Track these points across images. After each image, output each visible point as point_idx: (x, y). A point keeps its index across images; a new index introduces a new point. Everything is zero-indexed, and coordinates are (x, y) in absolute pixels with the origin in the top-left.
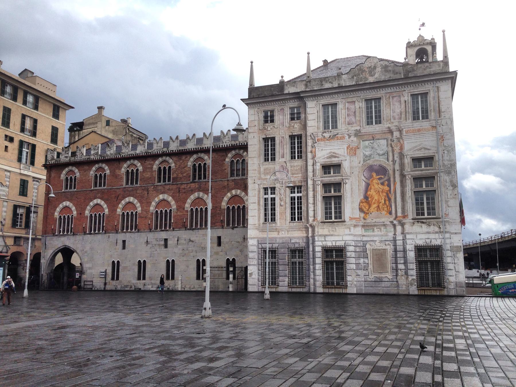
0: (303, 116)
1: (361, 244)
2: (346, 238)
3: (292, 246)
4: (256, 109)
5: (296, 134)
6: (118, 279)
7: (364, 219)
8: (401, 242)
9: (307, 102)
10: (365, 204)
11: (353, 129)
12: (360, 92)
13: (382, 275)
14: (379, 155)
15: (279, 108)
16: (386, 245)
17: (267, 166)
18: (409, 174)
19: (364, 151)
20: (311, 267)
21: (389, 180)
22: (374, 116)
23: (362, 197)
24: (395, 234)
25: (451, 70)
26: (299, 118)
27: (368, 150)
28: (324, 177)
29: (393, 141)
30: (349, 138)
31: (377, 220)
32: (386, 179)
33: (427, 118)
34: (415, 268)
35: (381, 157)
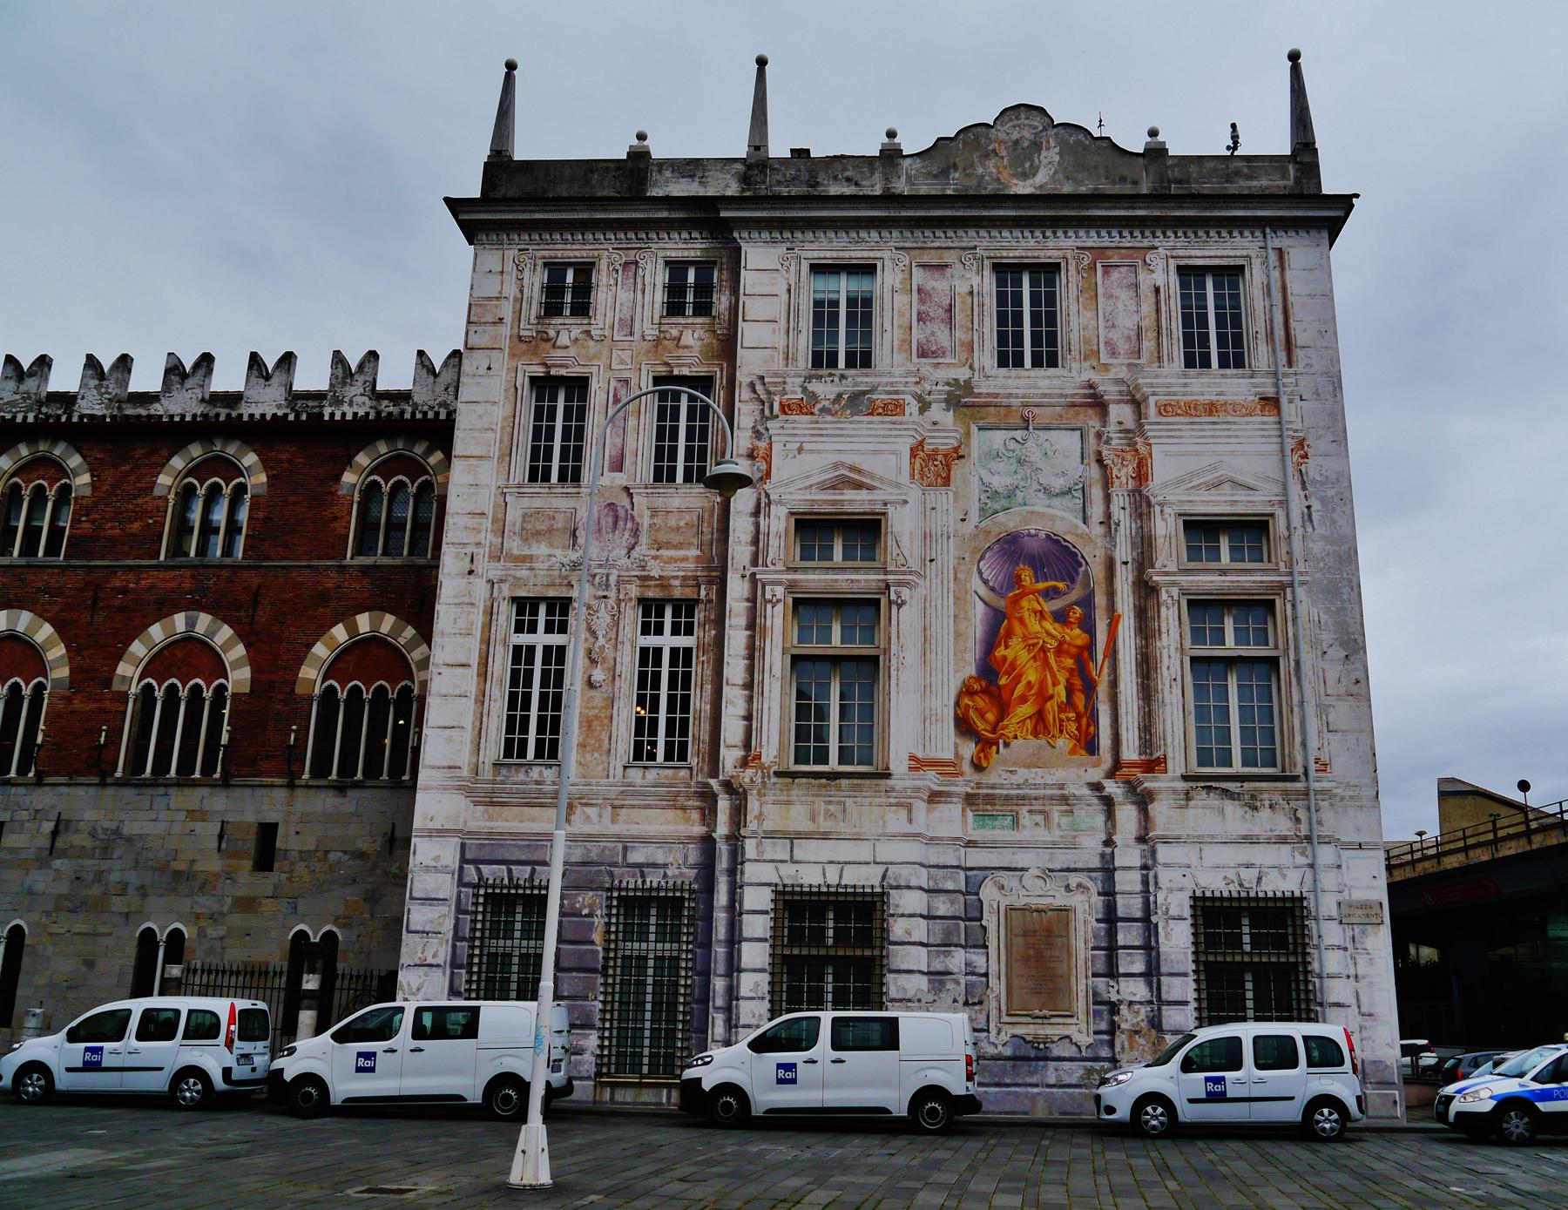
0: (721, 302)
1: (958, 882)
2: (888, 851)
3: (631, 881)
4: (512, 253)
7: (978, 767)
8: (1136, 876)
9: (745, 247)
10: (981, 702)
11: (943, 374)
12: (972, 233)
13: (1049, 1030)
15: (620, 258)
16: (1068, 889)
17: (537, 503)
18: (1174, 584)
19: (984, 473)
20: (719, 984)
21: (1087, 602)
22: (1028, 331)
23: (971, 670)
24: (1109, 842)
25: (1328, 188)
26: (703, 309)
27: (1001, 466)
28: (805, 570)
29: (1107, 442)
30: (922, 410)
32: (1074, 595)
33: (1239, 364)
34: (1191, 995)
35: (1056, 502)
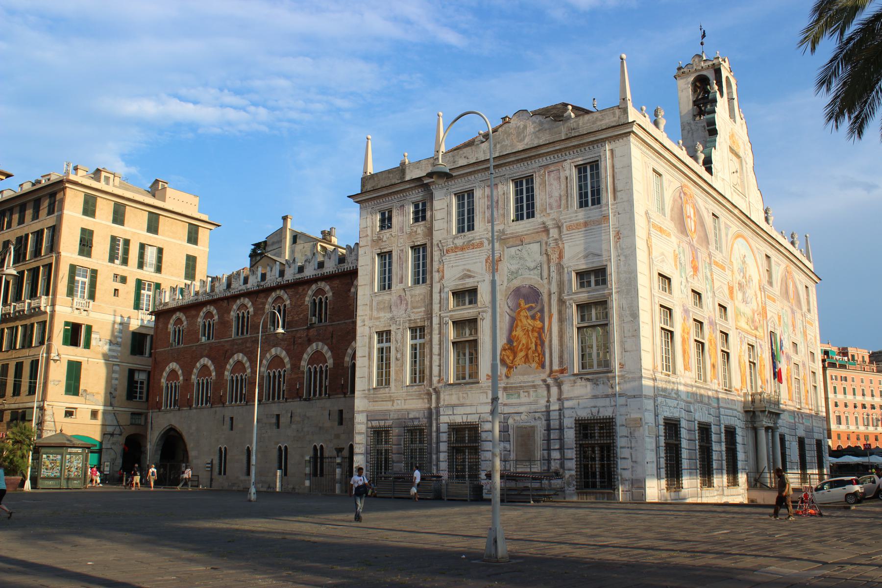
0: (428, 214)
3: (410, 424)
5: (419, 243)
6: (225, 474)
7: (507, 377)
8: (557, 413)
10: (508, 352)
12: (504, 169)
14: (529, 269)
15: (399, 204)
17: (380, 298)
18: (571, 299)
20: (434, 457)
21: (542, 311)
24: (548, 401)
26: (424, 218)
31: (526, 378)
32: (538, 308)
34: (574, 456)
35: (532, 272)
